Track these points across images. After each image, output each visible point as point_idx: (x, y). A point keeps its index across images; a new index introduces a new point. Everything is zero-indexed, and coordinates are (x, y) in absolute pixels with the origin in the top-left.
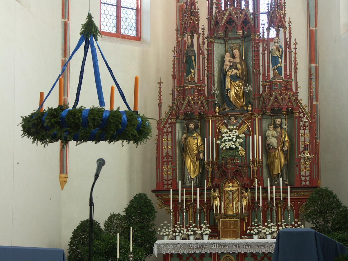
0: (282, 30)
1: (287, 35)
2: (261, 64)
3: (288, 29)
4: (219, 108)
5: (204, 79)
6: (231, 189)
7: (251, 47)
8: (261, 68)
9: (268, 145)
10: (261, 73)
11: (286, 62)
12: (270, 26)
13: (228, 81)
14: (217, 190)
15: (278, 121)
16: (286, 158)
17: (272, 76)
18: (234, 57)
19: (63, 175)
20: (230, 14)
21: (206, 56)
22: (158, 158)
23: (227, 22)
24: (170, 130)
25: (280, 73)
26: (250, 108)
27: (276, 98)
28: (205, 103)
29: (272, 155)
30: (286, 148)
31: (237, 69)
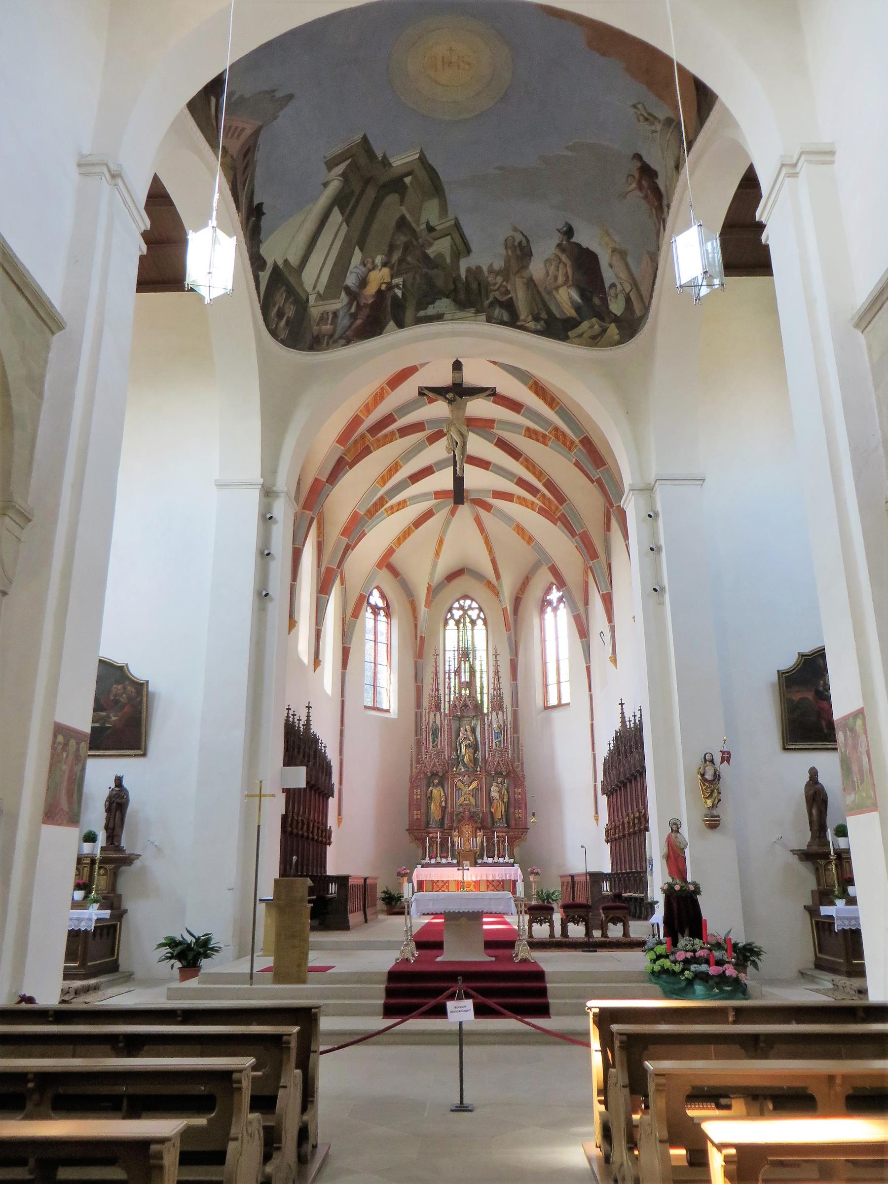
0: (500, 713)
1: (505, 718)
2: (487, 737)
3: (505, 713)
4: (456, 768)
5: (445, 746)
6: (467, 829)
7: (479, 724)
8: (487, 740)
9: (492, 797)
10: (487, 743)
11: (504, 736)
12: (492, 710)
13: (464, 750)
14: (457, 831)
15: (499, 780)
16: (505, 807)
17: (494, 746)
18: (466, 731)
19: (340, 817)
20: (465, 700)
21: (446, 729)
22: (410, 805)
23: (463, 706)
24: (419, 784)
25: (500, 745)
26: (478, 769)
27: (499, 763)
28: (446, 764)
29: (495, 805)
30: (505, 800)
31: (470, 740)
